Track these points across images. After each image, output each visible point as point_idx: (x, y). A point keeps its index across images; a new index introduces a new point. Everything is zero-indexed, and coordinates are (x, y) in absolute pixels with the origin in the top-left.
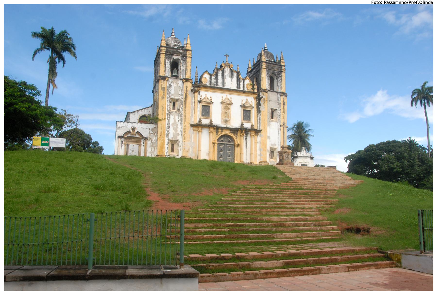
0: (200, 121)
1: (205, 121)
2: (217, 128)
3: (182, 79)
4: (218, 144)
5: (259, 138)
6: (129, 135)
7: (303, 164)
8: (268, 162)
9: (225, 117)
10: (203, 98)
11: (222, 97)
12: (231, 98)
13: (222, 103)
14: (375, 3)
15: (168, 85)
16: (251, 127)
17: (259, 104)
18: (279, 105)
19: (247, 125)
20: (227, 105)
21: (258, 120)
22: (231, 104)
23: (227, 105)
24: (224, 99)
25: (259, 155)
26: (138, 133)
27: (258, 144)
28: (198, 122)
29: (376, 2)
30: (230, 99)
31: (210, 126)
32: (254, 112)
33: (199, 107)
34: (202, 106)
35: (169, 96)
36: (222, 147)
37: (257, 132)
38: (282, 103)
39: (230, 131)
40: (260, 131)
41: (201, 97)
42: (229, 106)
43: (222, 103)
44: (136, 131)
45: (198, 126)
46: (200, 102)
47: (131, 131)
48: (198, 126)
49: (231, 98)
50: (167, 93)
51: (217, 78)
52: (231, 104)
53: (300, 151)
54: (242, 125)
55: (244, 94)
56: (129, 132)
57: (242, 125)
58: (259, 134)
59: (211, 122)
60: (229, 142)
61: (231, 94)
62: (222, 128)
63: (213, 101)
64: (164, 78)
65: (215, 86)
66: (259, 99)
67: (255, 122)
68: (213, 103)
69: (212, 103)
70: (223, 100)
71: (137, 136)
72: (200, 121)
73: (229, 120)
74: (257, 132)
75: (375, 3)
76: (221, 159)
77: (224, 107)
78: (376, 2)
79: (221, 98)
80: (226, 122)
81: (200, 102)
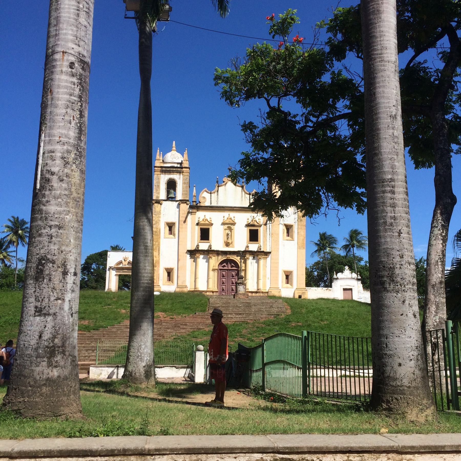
1: (204, 246)
2: (218, 253)
3: (178, 201)
4: (220, 270)
6: (121, 266)
7: (345, 287)
8: (279, 289)
9: (227, 239)
10: (201, 220)
11: (224, 217)
12: (234, 217)
19: (253, 247)
24: (226, 218)
30: (233, 219)
33: (197, 230)
36: (224, 273)
37: (267, 254)
40: (270, 253)
41: (199, 219)
42: (232, 227)
43: (223, 224)
46: (198, 224)
47: (123, 261)
52: (234, 224)
53: (342, 272)
56: (121, 262)
59: (210, 246)
60: (232, 267)
63: (212, 223)
68: (212, 224)
69: (212, 224)
70: (225, 220)
73: (232, 243)
74: (267, 254)
76: (223, 286)
77: (226, 228)
79: (223, 218)
80: (227, 244)
81: (198, 224)
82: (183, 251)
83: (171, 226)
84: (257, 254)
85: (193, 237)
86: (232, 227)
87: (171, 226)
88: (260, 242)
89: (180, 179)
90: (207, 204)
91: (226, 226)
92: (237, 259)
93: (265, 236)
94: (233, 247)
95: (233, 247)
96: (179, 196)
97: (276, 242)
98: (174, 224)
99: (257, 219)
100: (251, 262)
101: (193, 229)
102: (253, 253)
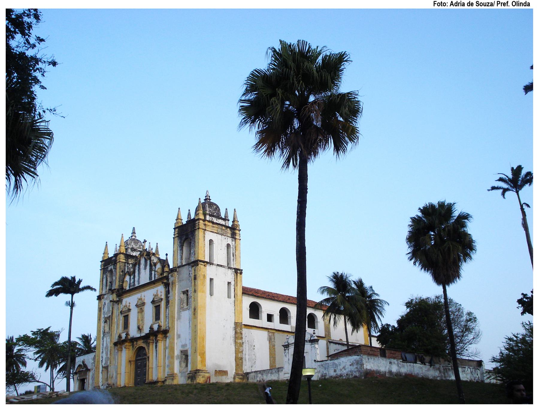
14: (439, 4)
15: (103, 304)
17: (168, 293)
18: (191, 282)
21: (167, 315)
25: (168, 366)
27: (167, 351)
28: (117, 338)
29: (440, 2)
32: (163, 304)
34: (124, 316)
35: (104, 316)
38: (193, 278)
39: (142, 341)
50: (102, 313)
51: (134, 278)
55: (155, 285)
61: (144, 291)
65: (133, 287)
66: (167, 285)
67: (164, 319)
75: (439, 4)
78: (440, 2)
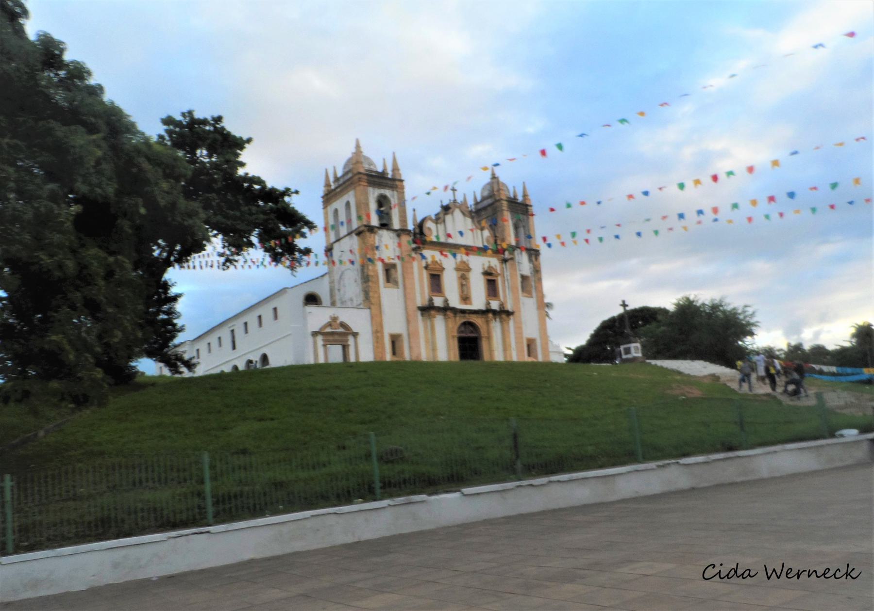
0: (431, 300)
2: (455, 311)
5: (511, 323)
6: (328, 330)
13: (457, 269)
16: (500, 308)
19: (495, 305)
20: (463, 271)
22: (469, 270)
23: (463, 271)
26: (343, 325)
31: (446, 309)
42: (466, 273)
44: (338, 322)
45: (427, 310)
48: (427, 310)
49: (468, 261)
54: (488, 304)
57: (488, 304)
58: (511, 317)
59: (446, 301)
60: (472, 332)
62: (463, 312)
64: (371, 229)
71: (341, 330)
72: (431, 300)
74: (509, 314)
82: (413, 308)
83: (389, 269)
84: (503, 313)
85: (422, 287)
86: (466, 273)
87: (389, 269)
88: (499, 297)
89: (393, 196)
90: (435, 240)
91: (461, 273)
92: (478, 320)
93: (504, 291)
94: (471, 304)
95: (471, 304)
96: (396, 225)
97: (516, 301)
98: (394, 266)
99: (492, 264)
100: (496, 327)
101: (421, 274)
102: (495, 312)
